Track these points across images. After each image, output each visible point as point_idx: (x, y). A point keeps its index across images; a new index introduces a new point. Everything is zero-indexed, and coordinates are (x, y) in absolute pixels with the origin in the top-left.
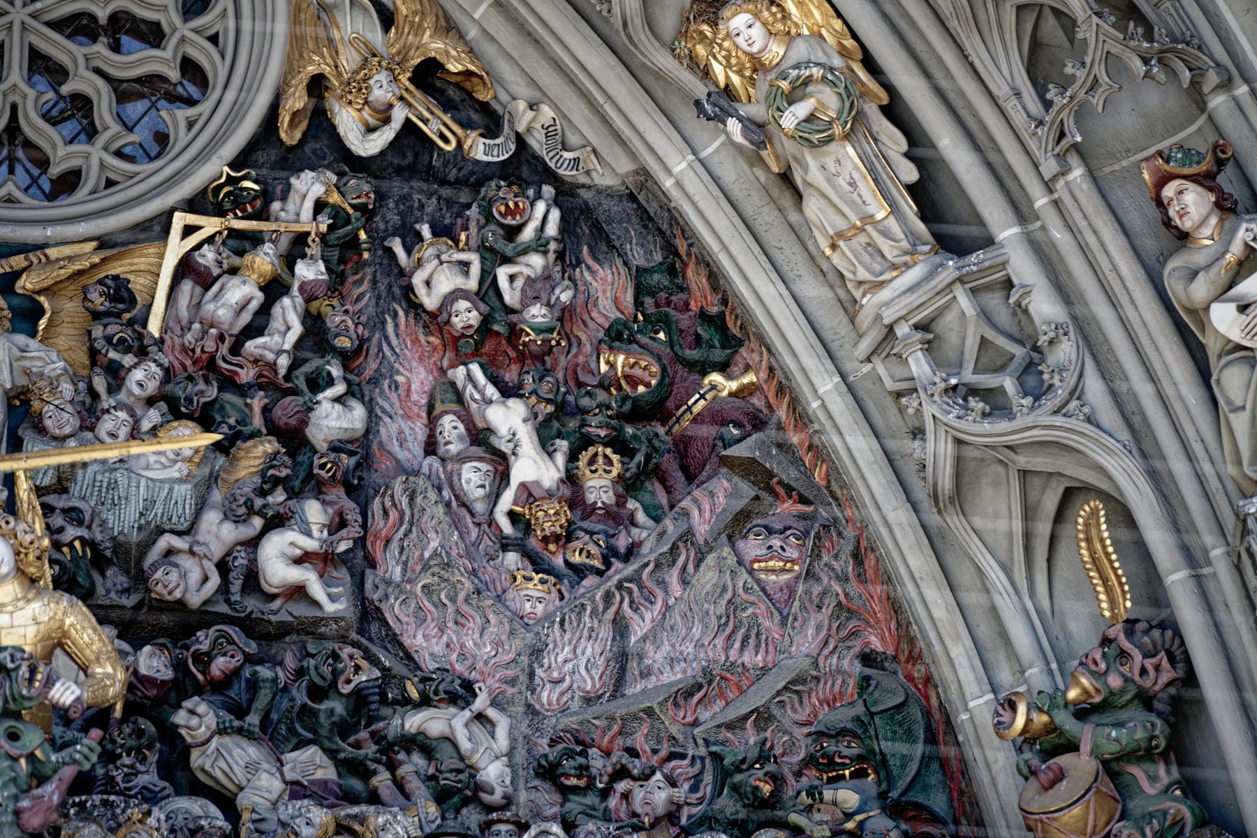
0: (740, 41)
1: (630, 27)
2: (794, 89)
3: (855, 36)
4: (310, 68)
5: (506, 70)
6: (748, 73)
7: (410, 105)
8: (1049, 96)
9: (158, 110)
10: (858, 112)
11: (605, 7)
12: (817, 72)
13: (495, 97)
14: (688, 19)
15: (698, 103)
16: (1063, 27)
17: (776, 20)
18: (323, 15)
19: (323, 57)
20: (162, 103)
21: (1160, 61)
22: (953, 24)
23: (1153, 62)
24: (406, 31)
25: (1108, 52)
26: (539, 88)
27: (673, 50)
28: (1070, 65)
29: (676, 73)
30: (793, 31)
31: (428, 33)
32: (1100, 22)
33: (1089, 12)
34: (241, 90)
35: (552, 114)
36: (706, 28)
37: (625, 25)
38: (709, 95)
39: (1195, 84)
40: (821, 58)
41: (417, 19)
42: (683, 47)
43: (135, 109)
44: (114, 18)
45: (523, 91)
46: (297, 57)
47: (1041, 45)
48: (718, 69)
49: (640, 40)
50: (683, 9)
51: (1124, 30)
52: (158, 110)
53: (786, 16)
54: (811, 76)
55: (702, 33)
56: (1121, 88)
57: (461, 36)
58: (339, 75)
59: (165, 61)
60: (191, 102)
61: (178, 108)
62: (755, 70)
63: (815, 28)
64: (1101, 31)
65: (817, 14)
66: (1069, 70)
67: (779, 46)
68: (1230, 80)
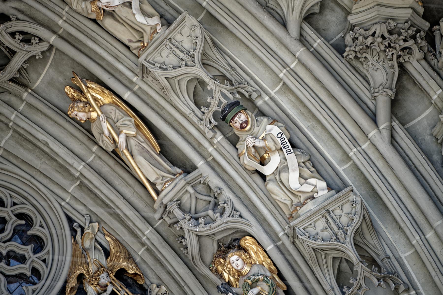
0: (234, 265)
1: (194, 259)
2: (253, 283)
3: (275, 265)
4: (78, 271)
5: (149, 273)
6: (236, 277)
7: (114, 285)
8: (344, 290)
9: (22, 286)
10: (275, 292)
11: (186, 251)
12: (261, 277)
13: (145, 283)
14: (215, 257)
15: (218, 287)
16: (349, 266)
17: (247, 258)
18: (84, 253)
19: (83, 268)
20: (24, 284)
21: (384, 280)
22: (310, 262)
23: (381, 280)
24: (114, 258)
25: (365, 276)
26: (161, 280)
27: (210, 268)
28: (352, 279)
29: (211, 276)
30: (253, 263)
31: (122, 259)
32: (362, 265)
33: (358, 261)
34: (52, 281)
35: (165, 289)
36: (222, 260)
37: (193, 258)
38: (222, 284)
39: (396, 289)
40: (263, 273)
41: (118, 254)
42: (213, 267)
43: (13, 286)
44: (8, 253)
45: (155, 280)
46: (74, 267)
47: (341, 272)
48: (226, 275)
49: (198, 263)
50: (214, 253)
51: (371, 268)
52: (22, 286)
53: (250, 257)
54: (259, 279)
55: (220, 262)
56: (370, 289)
57: (134, 261)
58: (89, 274)
59: (26, 269)
60: (34, 284)
61: (29, 286)
62: (239, 276)
63: (261, 262)
64: (362, 268)
65: (261, 257)
66: (351, 281)
67: (248, 267)
68: (409, 288)
